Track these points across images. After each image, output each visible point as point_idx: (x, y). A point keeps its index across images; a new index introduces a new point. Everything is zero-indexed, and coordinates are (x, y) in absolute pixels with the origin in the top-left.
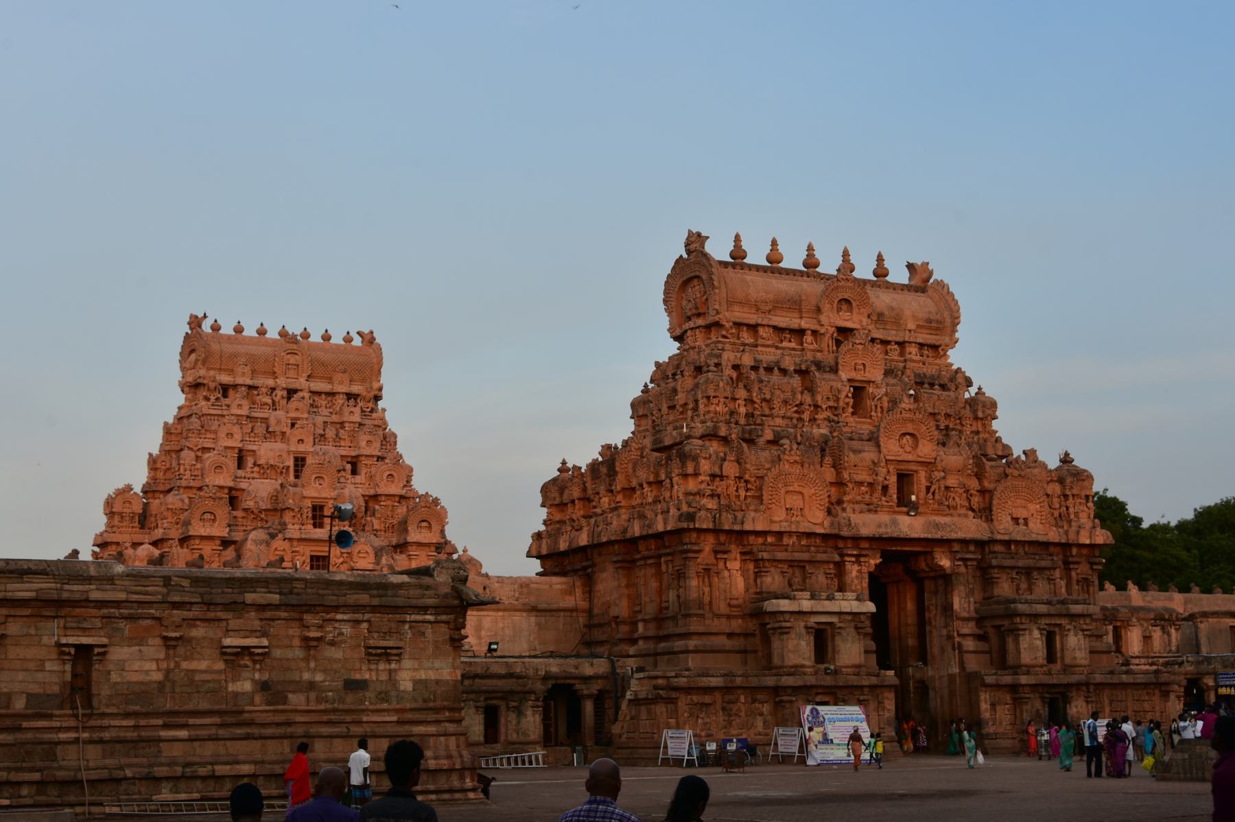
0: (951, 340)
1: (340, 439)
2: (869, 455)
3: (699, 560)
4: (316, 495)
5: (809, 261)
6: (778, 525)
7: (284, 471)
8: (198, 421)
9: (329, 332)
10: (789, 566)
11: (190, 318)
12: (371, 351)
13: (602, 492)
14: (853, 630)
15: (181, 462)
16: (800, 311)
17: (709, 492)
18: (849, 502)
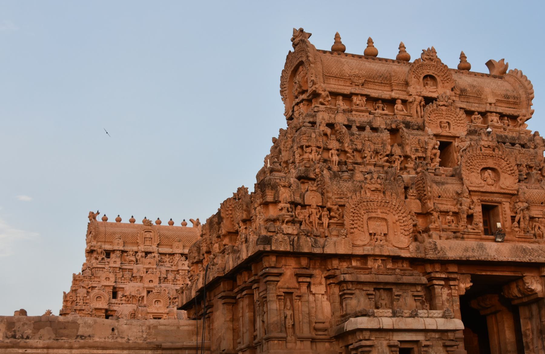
0: (527, 111)
1: (177, 280)
2: (453, 187)
3: (279, 284)
4: (156, 311)
5: (401, 55)
6: (361, 248)
7: (141, 299)
8: (90, 272)
9: (173, 220)
10: (375, 289)
11: (90, 214)
12: (197, 229)
13: (214, 239)
14: (441, 349)
15: (78, 295)
16: (391, 85)
17: (288, 218)
18: (436, 229)
